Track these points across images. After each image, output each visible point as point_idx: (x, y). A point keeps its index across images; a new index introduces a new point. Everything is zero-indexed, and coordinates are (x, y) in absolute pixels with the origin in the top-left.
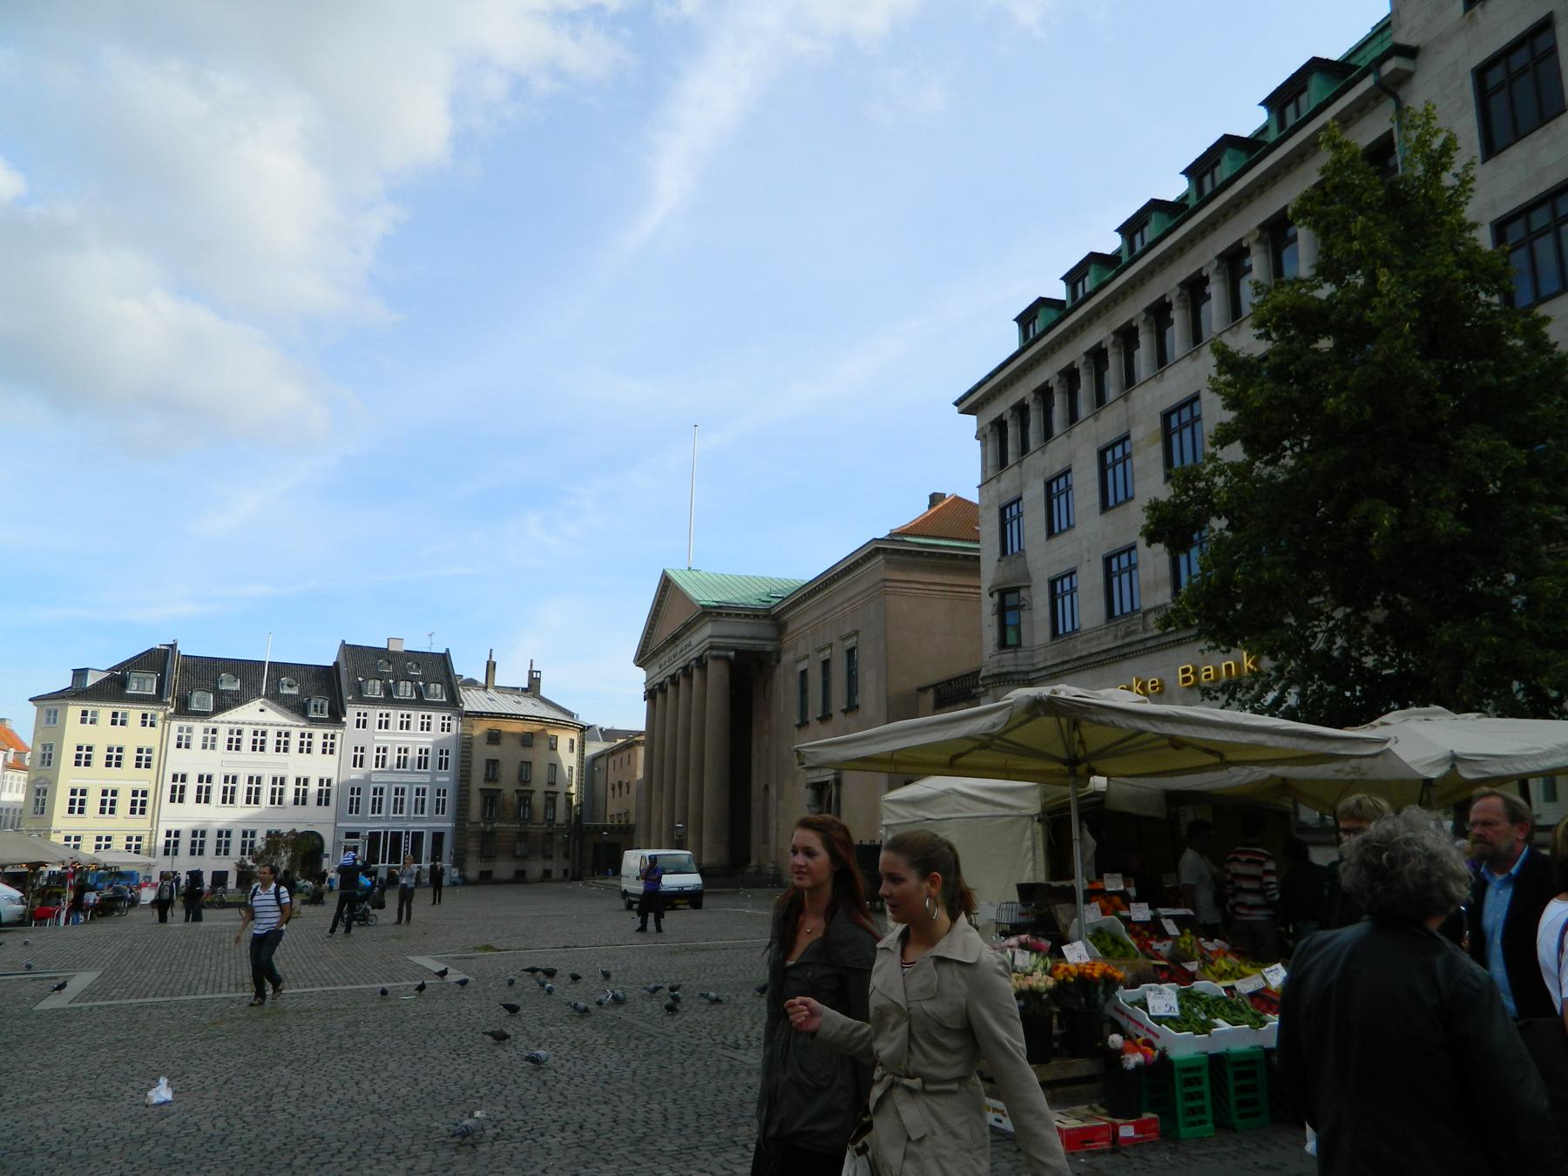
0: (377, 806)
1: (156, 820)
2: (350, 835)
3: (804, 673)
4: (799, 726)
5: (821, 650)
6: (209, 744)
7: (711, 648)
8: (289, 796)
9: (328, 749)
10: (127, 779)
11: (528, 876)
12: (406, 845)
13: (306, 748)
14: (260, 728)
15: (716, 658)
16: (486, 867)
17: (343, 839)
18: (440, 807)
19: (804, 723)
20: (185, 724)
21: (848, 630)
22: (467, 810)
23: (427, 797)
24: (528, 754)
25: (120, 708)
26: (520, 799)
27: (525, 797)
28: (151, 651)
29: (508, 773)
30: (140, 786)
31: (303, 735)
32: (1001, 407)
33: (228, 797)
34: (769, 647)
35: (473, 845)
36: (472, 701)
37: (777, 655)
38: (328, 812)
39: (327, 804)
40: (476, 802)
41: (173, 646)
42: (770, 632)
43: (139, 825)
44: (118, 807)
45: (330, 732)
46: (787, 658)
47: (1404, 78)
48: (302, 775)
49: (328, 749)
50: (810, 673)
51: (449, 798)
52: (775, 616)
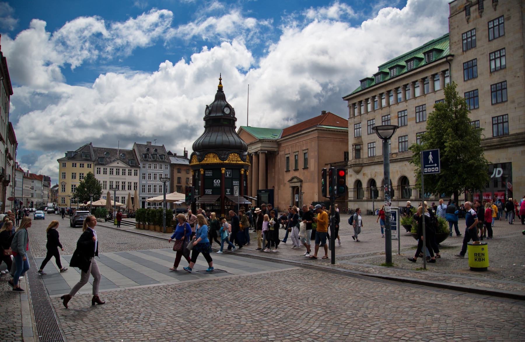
2: (143, 198)
3: (288, 158)
4: (286, 171)
5: (294, 152)
6: (105, 173)
7: (261, 150)
8: (114, 187)
9: (136, 174)
13: (130, 174)
14: (118, 168)
15: (262, 153)
17: (141, 199)
19: (288, 171)
20: (99, 167)
21: (304, 148)
25: (82, 162)
28: (86, 146)
29: (183, 180)
32: (356, 101)
34: (276, 150)
36: (173, 161)
37: (278, 151)
41: (91, 144)
42: (276, 146)
45: (136, 169)
46: (281, 153)
47: (451, 60)
49: (136, 174)
50: (290, 158)
52: (278, 143)
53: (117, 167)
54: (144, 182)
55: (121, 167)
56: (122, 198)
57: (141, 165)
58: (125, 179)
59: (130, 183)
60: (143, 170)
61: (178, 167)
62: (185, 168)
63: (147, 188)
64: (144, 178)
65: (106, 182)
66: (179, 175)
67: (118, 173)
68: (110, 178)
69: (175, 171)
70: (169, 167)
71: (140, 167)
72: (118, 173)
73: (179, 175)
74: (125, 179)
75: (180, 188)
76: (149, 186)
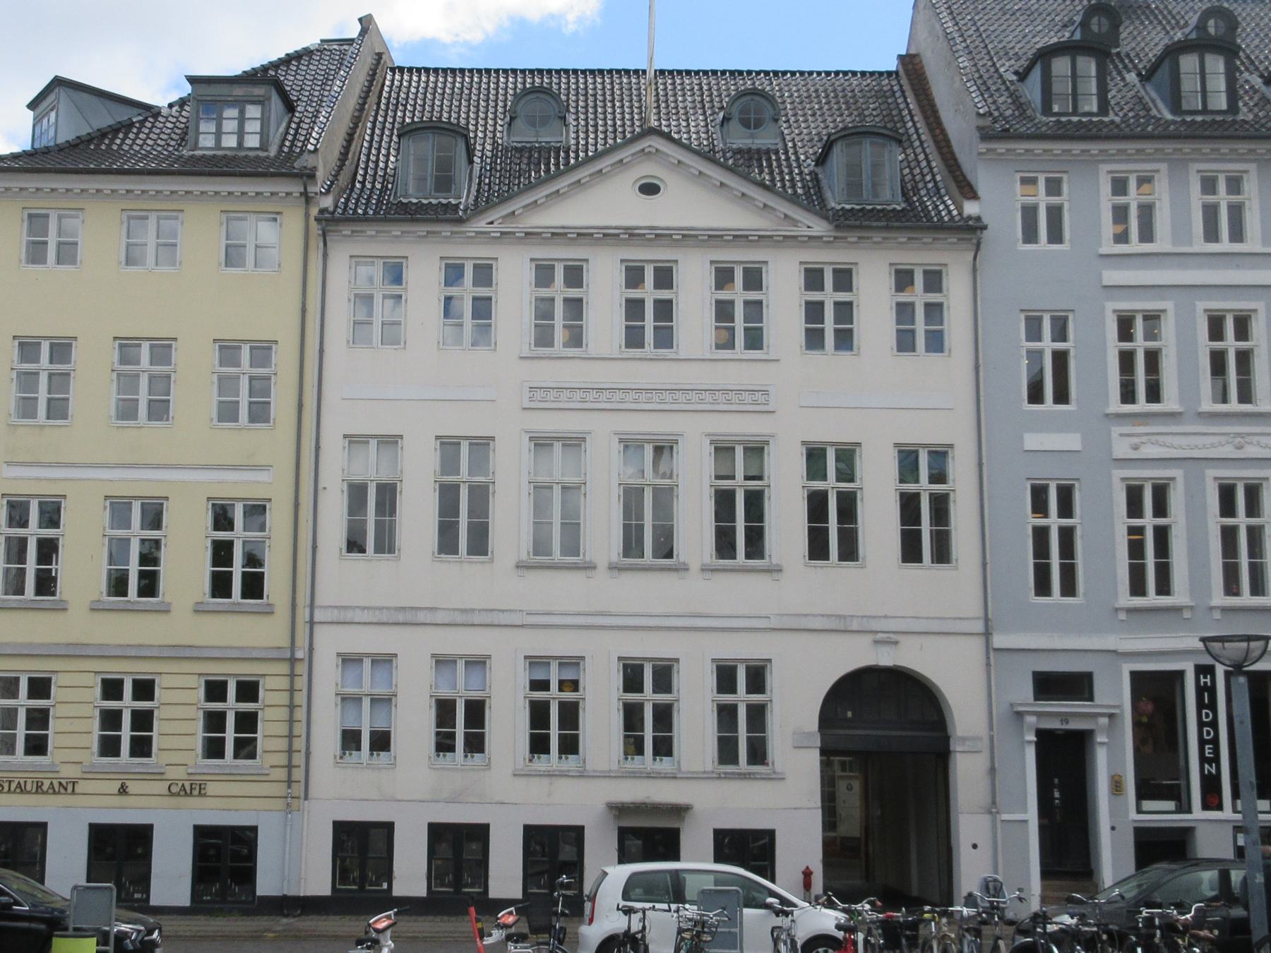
0: (1150, 563)
1: (305, 617)
2: (1052, 685)
9: (919, 331)
10: (194, 461)
30: (238, 486)
31: (813, 279)
38: (950, 589)
39: (942, 554)
43: (243, 633)
44: (64, 567)
45: (919, 257)
48: (829, 432)
49: (919, 331)
53: (632, 235)
54: (1051, 438)
55: (688, 238)
57: (999, 196)
58: (757, 400)
59: (829, 461)
60: (1022, 271)
63: (1103, 534)
64: (1052, 383)
65: (481, 445)
67: (649, 323)
68: (541, 397)
71: (972, 229)
72: (649, 323)
76: (1148, 498)
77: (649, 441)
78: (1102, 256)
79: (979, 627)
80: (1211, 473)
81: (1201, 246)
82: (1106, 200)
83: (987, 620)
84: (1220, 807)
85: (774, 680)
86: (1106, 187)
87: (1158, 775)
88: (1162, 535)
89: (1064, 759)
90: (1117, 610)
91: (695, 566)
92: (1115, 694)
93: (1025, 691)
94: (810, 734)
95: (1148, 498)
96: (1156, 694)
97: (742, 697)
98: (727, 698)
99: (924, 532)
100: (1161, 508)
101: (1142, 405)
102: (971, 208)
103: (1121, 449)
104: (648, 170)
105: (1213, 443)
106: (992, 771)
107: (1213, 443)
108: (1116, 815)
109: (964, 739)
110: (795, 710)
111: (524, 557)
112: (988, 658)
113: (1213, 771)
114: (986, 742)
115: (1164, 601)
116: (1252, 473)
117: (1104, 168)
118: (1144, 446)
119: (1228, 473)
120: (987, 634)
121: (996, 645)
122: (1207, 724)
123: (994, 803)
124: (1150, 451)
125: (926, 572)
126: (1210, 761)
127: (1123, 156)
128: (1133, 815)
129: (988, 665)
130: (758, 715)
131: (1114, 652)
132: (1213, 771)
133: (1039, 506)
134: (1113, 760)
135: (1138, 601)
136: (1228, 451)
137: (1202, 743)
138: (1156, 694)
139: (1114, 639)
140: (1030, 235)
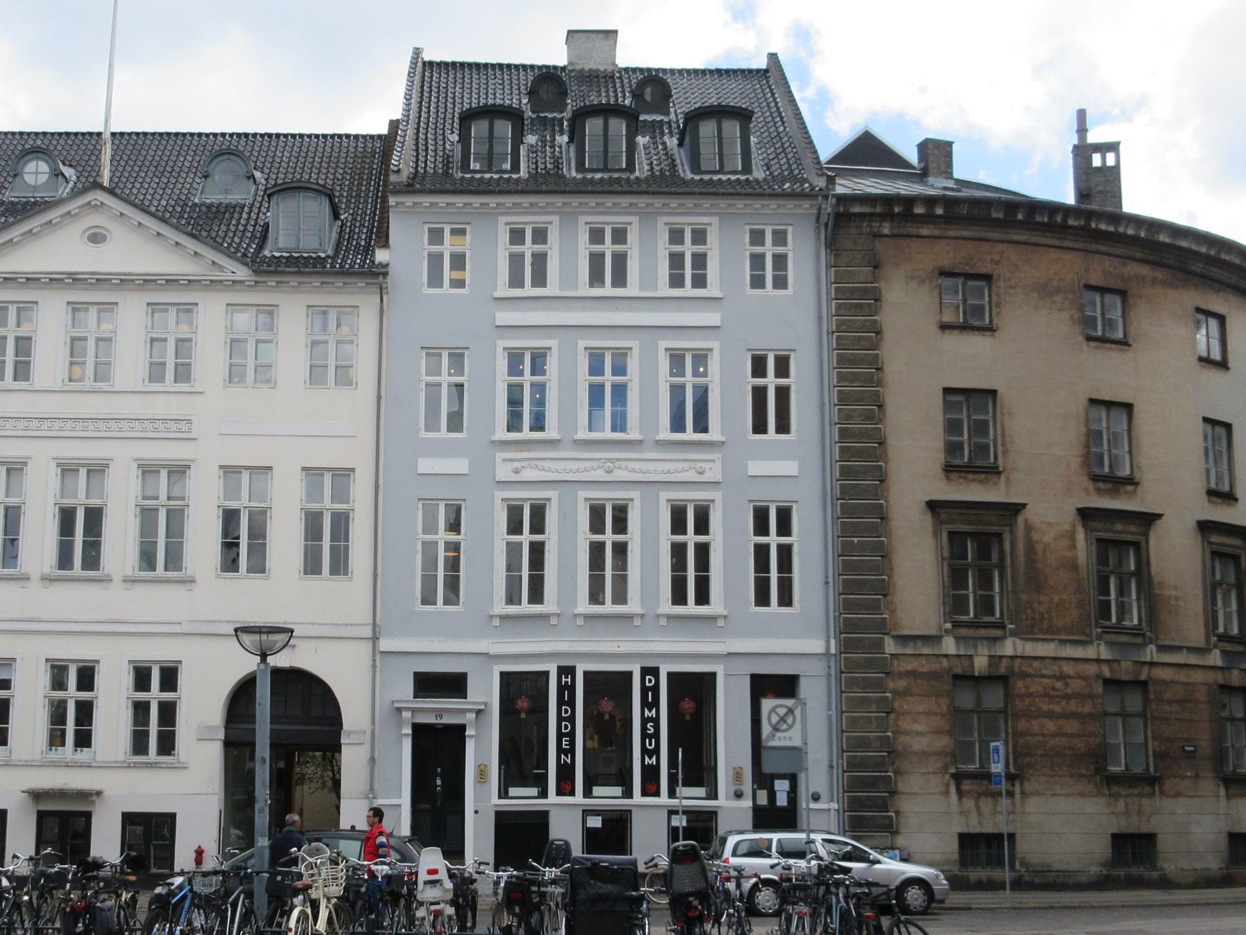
2: (428, 684)
11: (1171, 862)
12: (649, 727)
16: (991, 819)
18: (772, 580)
22: (884, 590)
23: (716, 537)
24: (1112, 374)
26: (1104, 546)
27: (1120, 536)
33: (160, 553)
35: (921, 729)
39: (340, 565)
40: (917, 564)
51: (811, 544)
55: (125, 282)
56: (142, 678)
58: (182, 429)
61: (946, 255)
62: (1065, 265)
66: (972, 360)
69: (908, 304)
70: (804, 255)
73: (972, 360)
74: (182, 429)
75: (987, 542)
77: (83, 465)
78: (496, 299)
79: (368, 632)
80: (583, 494)
81: (585, 290)
82: (584, 247)
83: (374, 625)
84: (572, 793)
85: (183, 679)
86: (504, 237)
87: (520, 762)
88: (703, 552)
89: (437, 752)
90: (491, 617)
91: (35, 576)
92: (485, 692)
93: (407, 688)
94: (211, 728)
95: (690, 518)
96: (522, 691)
97: (155, 695)
98: (142, 696)
99: (326, 545)
100: (538, 527)
101: (526, 434)
102: (381, 256)
103: (504, 472)
104: (94, 220)
105: (588, 467)
106: (372, 760)
107: (588, 467)
108: (483, 799)
109: (350, 733)
110: (202, 708)
111: (129, 572)
112: (374, 660)
113: (647, 759)
114: (368, 734)
115: (536, 609)
116: (619, 494)
117: (503, 220)
118: (526, 471)
119: (598, 494)
120: (375, 639)
121: (382, 649)
122: (565, 719)
123: (372, 789)
124: (529, 475)
125: (325, 584)
126: (566, 752)
127: (516, 209)
128: (495, 800)
129: (374, 666)
130: (168, 712)
131: (487, 654)
132: (647, 759)
133: (761, 526)
134: (482, 752)
135: (679, 610)
136: (598, 475)
137: (560, 736)
138: (522, 691)
139: (487, 643)
140: (435, 279)
